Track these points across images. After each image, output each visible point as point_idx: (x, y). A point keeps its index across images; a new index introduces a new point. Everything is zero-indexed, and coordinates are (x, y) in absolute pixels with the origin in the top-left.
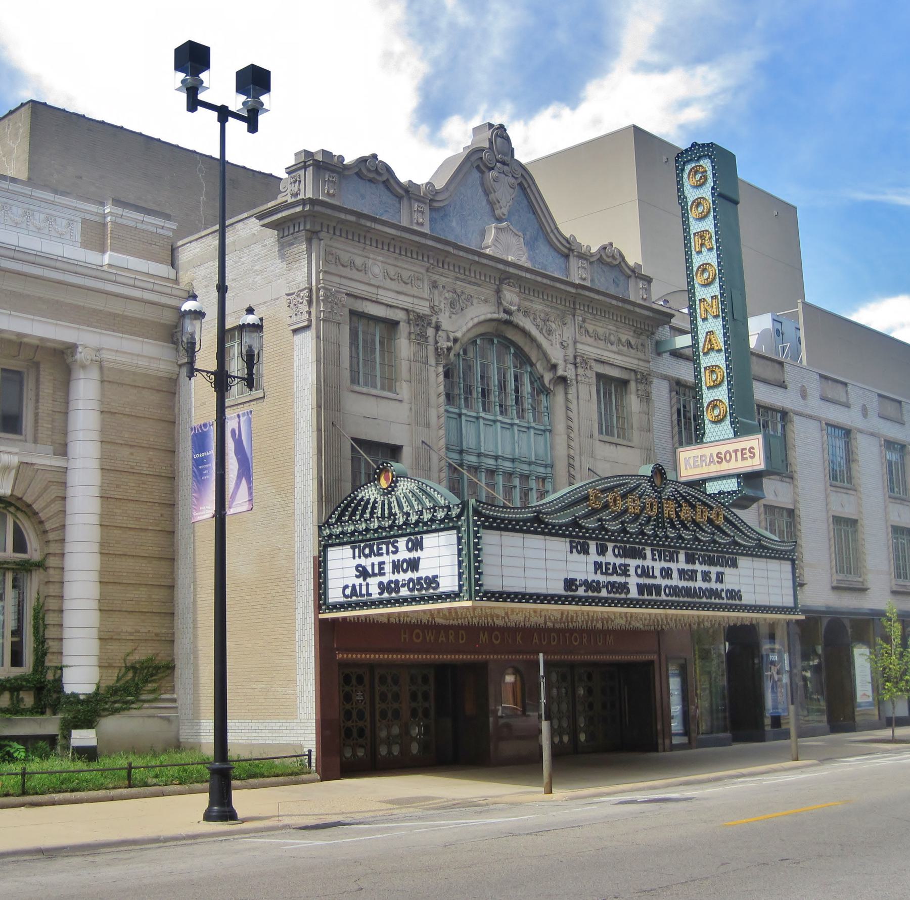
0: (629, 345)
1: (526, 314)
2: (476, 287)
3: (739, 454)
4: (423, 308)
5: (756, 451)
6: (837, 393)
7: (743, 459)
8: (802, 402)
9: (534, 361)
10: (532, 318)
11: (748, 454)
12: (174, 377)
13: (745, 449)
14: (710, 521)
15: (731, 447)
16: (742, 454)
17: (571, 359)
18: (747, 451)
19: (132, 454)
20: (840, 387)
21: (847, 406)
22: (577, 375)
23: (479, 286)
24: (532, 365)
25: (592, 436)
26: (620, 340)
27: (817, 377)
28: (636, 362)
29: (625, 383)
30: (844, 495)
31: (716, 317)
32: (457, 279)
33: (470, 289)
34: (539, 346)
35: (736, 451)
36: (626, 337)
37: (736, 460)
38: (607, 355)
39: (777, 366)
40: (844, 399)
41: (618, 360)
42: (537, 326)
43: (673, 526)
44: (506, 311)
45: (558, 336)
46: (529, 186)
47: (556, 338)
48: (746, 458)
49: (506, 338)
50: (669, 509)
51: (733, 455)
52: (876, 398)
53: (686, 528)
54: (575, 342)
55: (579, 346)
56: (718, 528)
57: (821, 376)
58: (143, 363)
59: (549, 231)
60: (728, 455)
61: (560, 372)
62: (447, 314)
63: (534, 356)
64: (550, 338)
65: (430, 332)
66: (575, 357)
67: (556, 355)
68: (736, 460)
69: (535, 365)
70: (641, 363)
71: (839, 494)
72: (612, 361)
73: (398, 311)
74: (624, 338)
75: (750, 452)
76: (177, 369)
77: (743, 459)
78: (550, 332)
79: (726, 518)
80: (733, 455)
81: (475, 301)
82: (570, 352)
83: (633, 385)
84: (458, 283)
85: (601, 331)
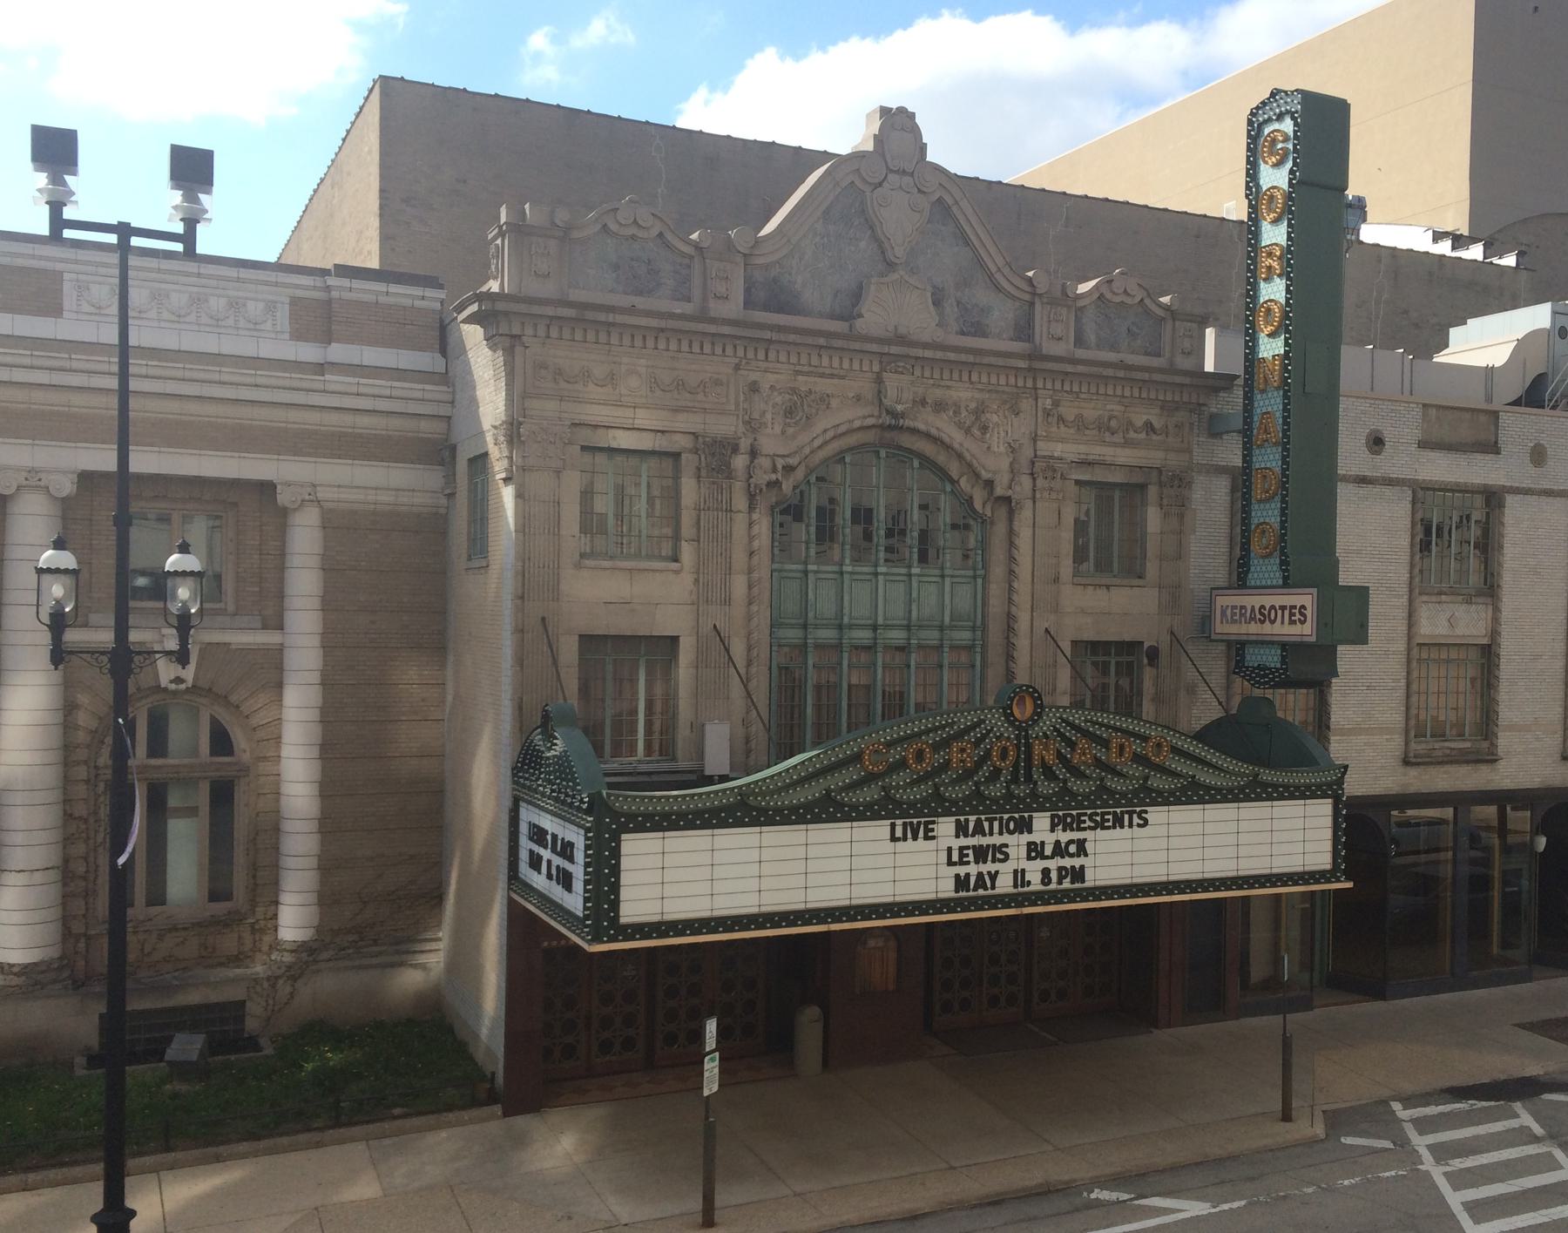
0: (1149, 427)
1: (939, 407)
2: (836, 381)
3: (1287, 613)
4: (724, 426)
5: (1308, 613)
8: (1532, 470)
12: (442, 511)
16: (1292, 614)
19: (373, 622)
23: (843, 378)
25: (1056, 580)
26: (1130, 423)
29: (1142, 487)
32: (798, 373)
33: (823, 386)
35: (1283, 608)
36: (1145, 418)
39: (1483, 418)
41: (1124, 456)
42: (960, 425)
53: (1081, 776)
54: (1035, 440)
58: (384, 498)
59: (994, 269)
61: (999, 491)
62: (778, 429)
63: (954, 469)
65: (740, 462)
72: (1109, 459)
73: (677, 437)
74: (1139, 421)
76: (444, 501)
77: (1292, 622)
78: (984, 429)
81: (834, 403)
83: (1153, 491)
84: (800, 378)
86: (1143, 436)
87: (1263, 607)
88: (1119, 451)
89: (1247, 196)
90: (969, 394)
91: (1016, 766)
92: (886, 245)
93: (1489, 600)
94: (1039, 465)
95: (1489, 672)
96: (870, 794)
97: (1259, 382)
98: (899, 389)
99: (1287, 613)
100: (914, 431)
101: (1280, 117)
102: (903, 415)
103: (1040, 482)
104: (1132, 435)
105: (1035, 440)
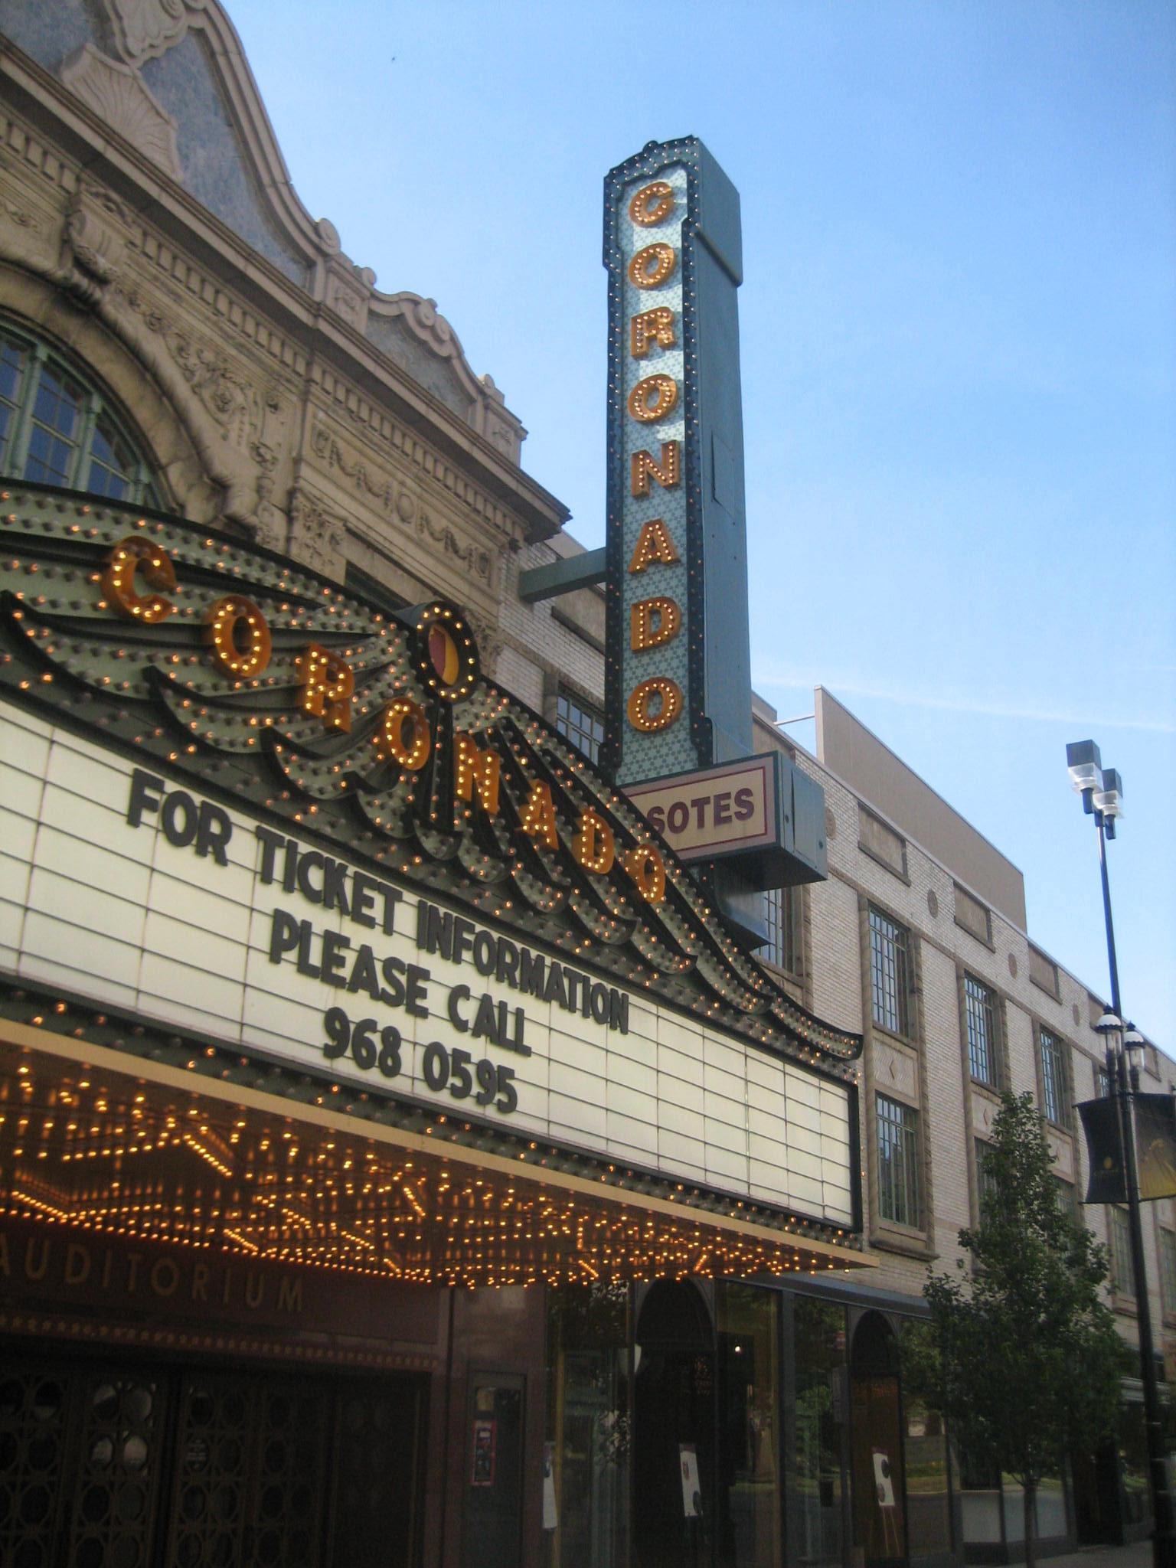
0: (451, 544)
1: (156, 323)
3: (709, 811)
5: (757, 800)
6: (891, 852)
7: (719, 820)
9: (164, 460)
10: (174, 342)
11: (734, 808)
13: (727, 796)
14: (619, 879)
15: (686, 794)
16: (719, 809)
17: (278, 496)
18: (732, 802)
20: (892, 842)
21: (904, 879)
22: (289, 540)
24: (156, 467)
27: (854, 804)
28: (465, 588)
30: (896, 1055)
31: (670, 488)
34: (180, 418)
36: (444, 523)
37: (701, 823)
38: (383, 532)
40: (899, 868)
42: (188, 372)
43: (486, 844)
44: (83, 266)
45: (247, 428)
46: (226, 53)
47: (240, 428)
48: (728, 819)
49: (76, 357)
50: (478, 777)
51: (693, 812)
52: (951, 889)
55: (305, 471)
56: (643, 909)
57: (862, 807)
59: (266, 180)
60: (678, 817)
64: (224, 417)
66: (291, 494)
67: (231, 459)
68: (701, 823)
69: (164, 468)
70: (476, 596)
71: (888, 1050)
72: (397, 554)
74: (439, 524)
75: (739, 802)
77: (719, 820)
79: (670, 891)
80: (693, 812)
82: (279, 482)
85: (377, 477)
86: (440, 546)
87: (659, 810)
88: (411, 549)
89: (606, 265)
90: (207, 331)
91: (424, 772)
92: (115, 26)
94: (300, 501)
96: (111, 671)
97: (633, 481)
98: (107, 237)
99: (709, 811)
100: (112, 333)
101: (662, 170)
102: (102, 281)
103: (298, 530)
104: (426, 536)
105: (297, 461)
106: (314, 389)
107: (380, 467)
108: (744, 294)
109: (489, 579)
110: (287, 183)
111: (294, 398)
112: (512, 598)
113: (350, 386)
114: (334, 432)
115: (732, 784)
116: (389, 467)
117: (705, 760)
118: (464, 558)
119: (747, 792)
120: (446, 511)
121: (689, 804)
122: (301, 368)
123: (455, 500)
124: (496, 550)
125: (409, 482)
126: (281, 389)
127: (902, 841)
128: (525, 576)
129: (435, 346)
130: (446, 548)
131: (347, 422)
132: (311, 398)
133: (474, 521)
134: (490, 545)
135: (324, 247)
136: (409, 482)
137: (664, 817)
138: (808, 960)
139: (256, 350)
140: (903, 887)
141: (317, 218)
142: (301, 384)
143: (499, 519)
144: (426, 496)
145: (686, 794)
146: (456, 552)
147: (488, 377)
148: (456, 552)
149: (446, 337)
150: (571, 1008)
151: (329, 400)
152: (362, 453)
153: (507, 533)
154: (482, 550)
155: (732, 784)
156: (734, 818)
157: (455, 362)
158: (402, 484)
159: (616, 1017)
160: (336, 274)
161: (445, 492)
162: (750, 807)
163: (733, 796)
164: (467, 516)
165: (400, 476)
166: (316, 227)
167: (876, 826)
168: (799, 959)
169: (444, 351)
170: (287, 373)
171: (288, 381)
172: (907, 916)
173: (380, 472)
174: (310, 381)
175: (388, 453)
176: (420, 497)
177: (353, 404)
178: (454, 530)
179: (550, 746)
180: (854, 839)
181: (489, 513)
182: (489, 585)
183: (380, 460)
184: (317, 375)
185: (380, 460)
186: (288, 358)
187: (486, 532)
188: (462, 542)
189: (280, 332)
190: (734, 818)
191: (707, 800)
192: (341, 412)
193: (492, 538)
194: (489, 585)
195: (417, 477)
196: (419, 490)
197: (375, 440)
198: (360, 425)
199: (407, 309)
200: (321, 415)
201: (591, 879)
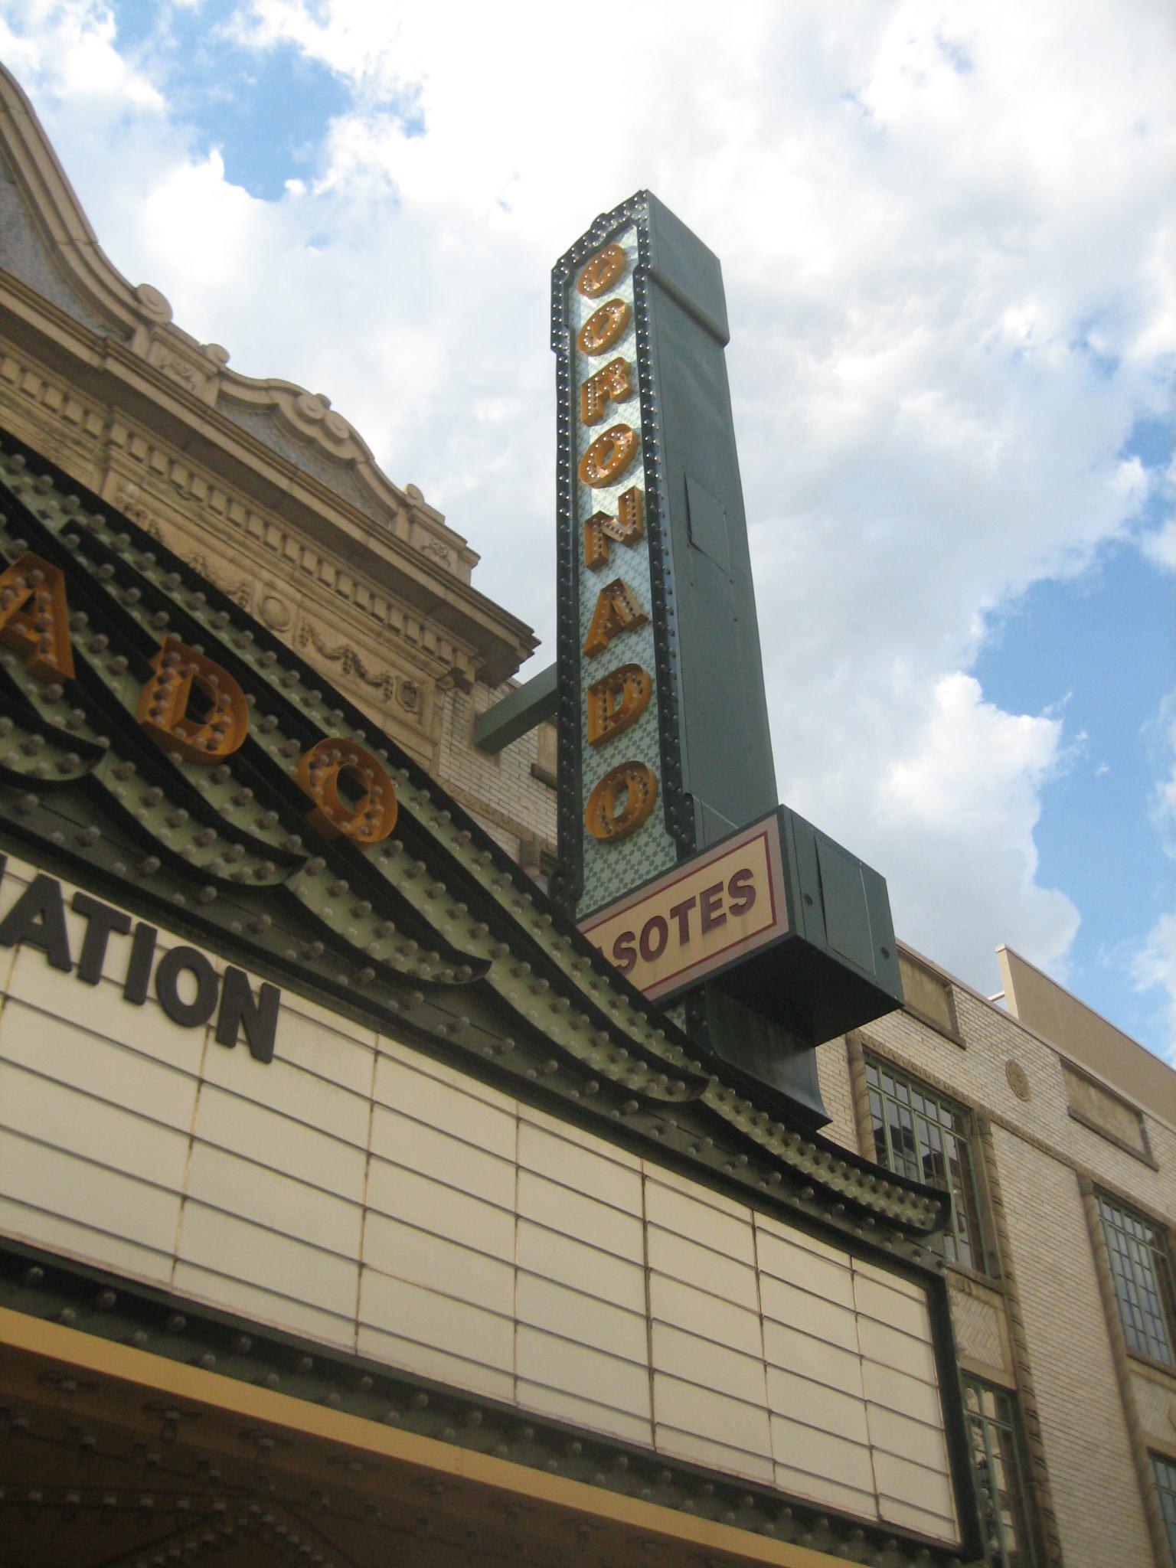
3: (695, 916)
5: (759, 882)
7: (709, 925)
11: (728, 901)
13: (718, 888)
15: (661, 905)
16: (709, 907)
18: (725, 895)
27: (1053, 1059)
36: (343, 641)
37: (684, 937)
40: (1139, 1146)
48: (721, 920)
51: (673, 926)
59: (58, 235)
68: (684, 937)
75: (735, 890)
77: (709, 925)
87: (628, 936)
93: (996, 1300)
95: (1025, 1451)
99: (695, 916)
106: (114, 452)
107: (232, 561)
108: (728, 349)
109: (420, 714)
110: (92, 243)
111: (90, 467)
112: (463, 746)
113: (174, 456)
114: (155, 512)
115: (722, 871)
116: (247, 562)
117: (686, 851)
118: (377, 685)
119: (745, 874)
120: (344, 625)
121: (666, 915)
122: (95, 426)
123: (355, 611)
124: (432, 682)
125: (280, 584)
126: (67, 452)
127: (1138, 1114)
128: (479, 719)
129: (329, 446)
130: (346, 670)
131: (175, 501)
132: (114, 465)
133: (389, 641)
134: (419, 674)
135: (144, 311)
136: (280, 584)
137: (635, 945)
138: (1006, 1255)
139: (22, 400)
140: (1148, 1172)
141: (135, 282)
142: (97, 446)
143: (429, 641)
144: (308, 603)
145: (661, 905)
146: (362, 675)
147: (411, 487)
148: (362, 675)
149: (344, 435)
150: (90, 972)
151: (141, 469)
152: (199, 540)
153: (447, 663)
154: (405, 678)
155: (722, 871)
156: (729, 916)
157: (363, 469)
158: (271, 585)
159: (248, 1026)
160: (163, 342)
161: (339, 601)
162: (750, 892)
163: (726, 886)
164: (379, 635)
165: (265, 575)
166: (133, 292)
167: (1093, 1092)
168: (992, 1255)
169: (346, 452)
170: (75, 433)
171: (77, 443)
172: (1161, 1209)
173: (231, 567)
174: (109, 443)
175: (242, 544)
176: (300, 606)
177: (180, 476)
178: (356, 648)
179: (82, 519)
180: (1061, 1104)
181: (413, 631)
182: (420, 722)
183: (231, 553)
184: (118, 434)
185: (231, 553)
186: (74, 412)
187: (413, 659)
188: (374, 667)
189: (61, 382)
190: (729, 916)
191: (690, 903)
192: (163, 486)
193: (424, 667)
194: (420, 722)
195: (292, 577)
196: (299, 596)
197: (221, 526)
198: (193, 504)
199: (284, 402)
200: (131, 488)
201: (176, 757)
